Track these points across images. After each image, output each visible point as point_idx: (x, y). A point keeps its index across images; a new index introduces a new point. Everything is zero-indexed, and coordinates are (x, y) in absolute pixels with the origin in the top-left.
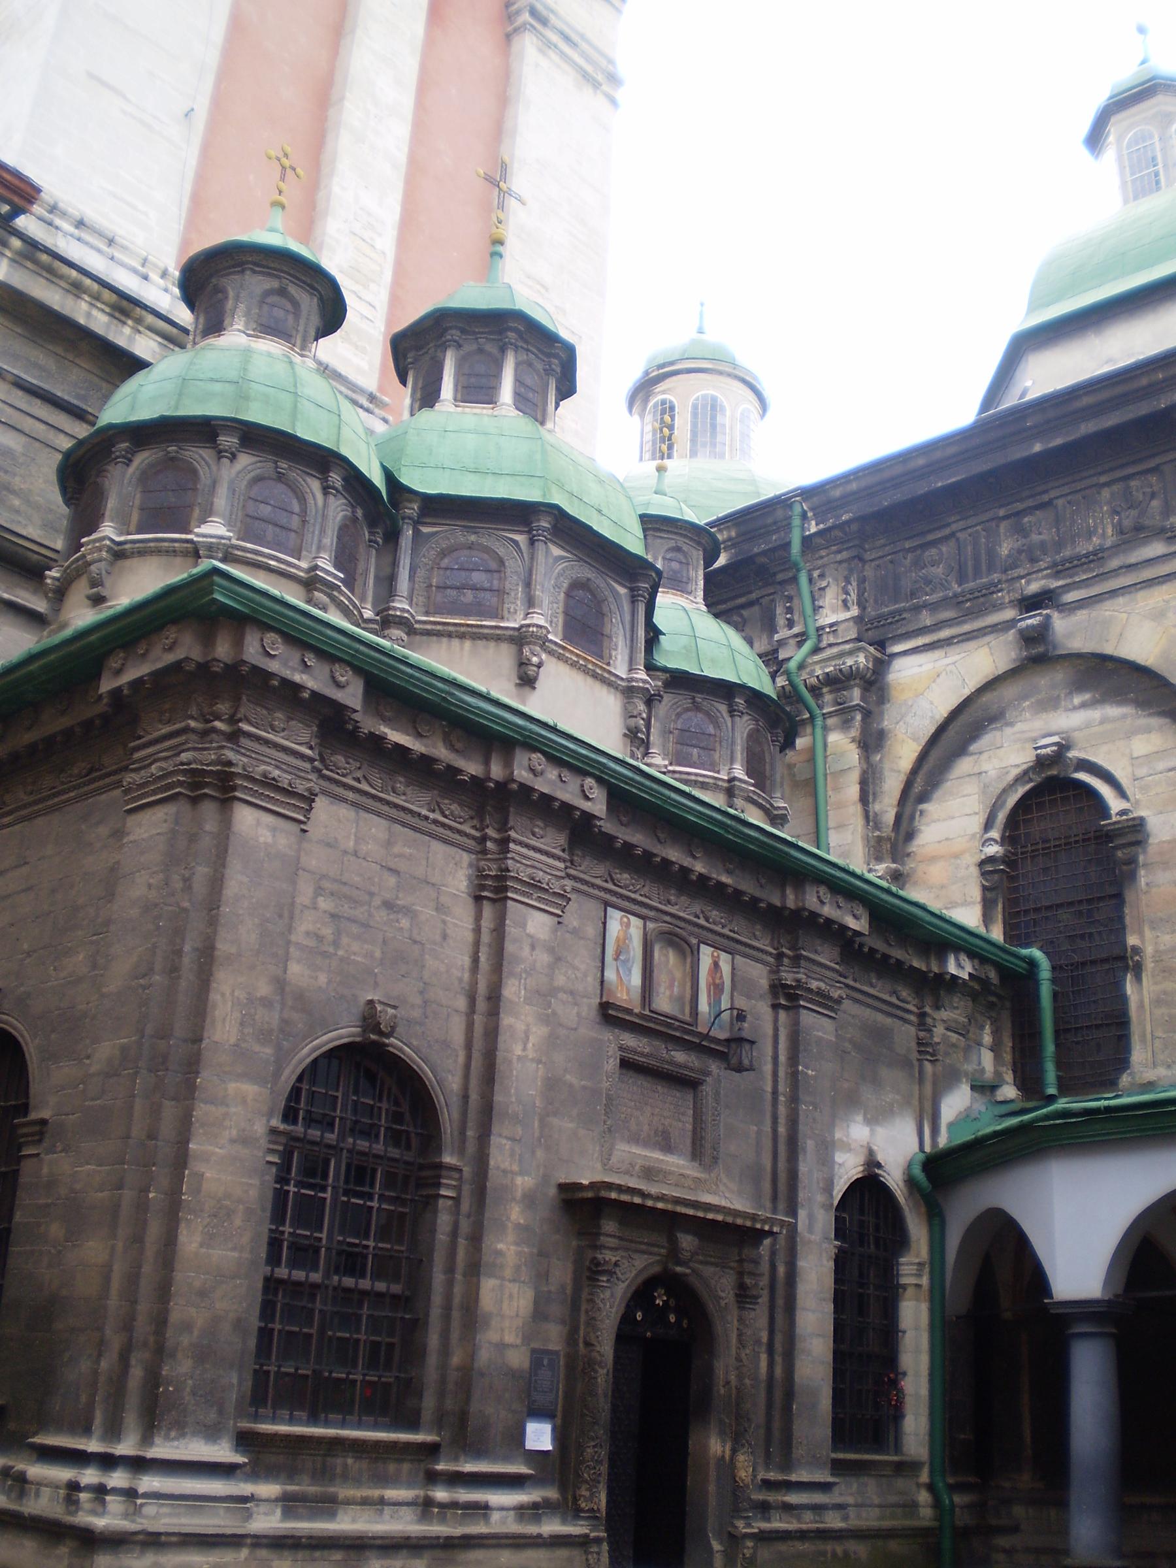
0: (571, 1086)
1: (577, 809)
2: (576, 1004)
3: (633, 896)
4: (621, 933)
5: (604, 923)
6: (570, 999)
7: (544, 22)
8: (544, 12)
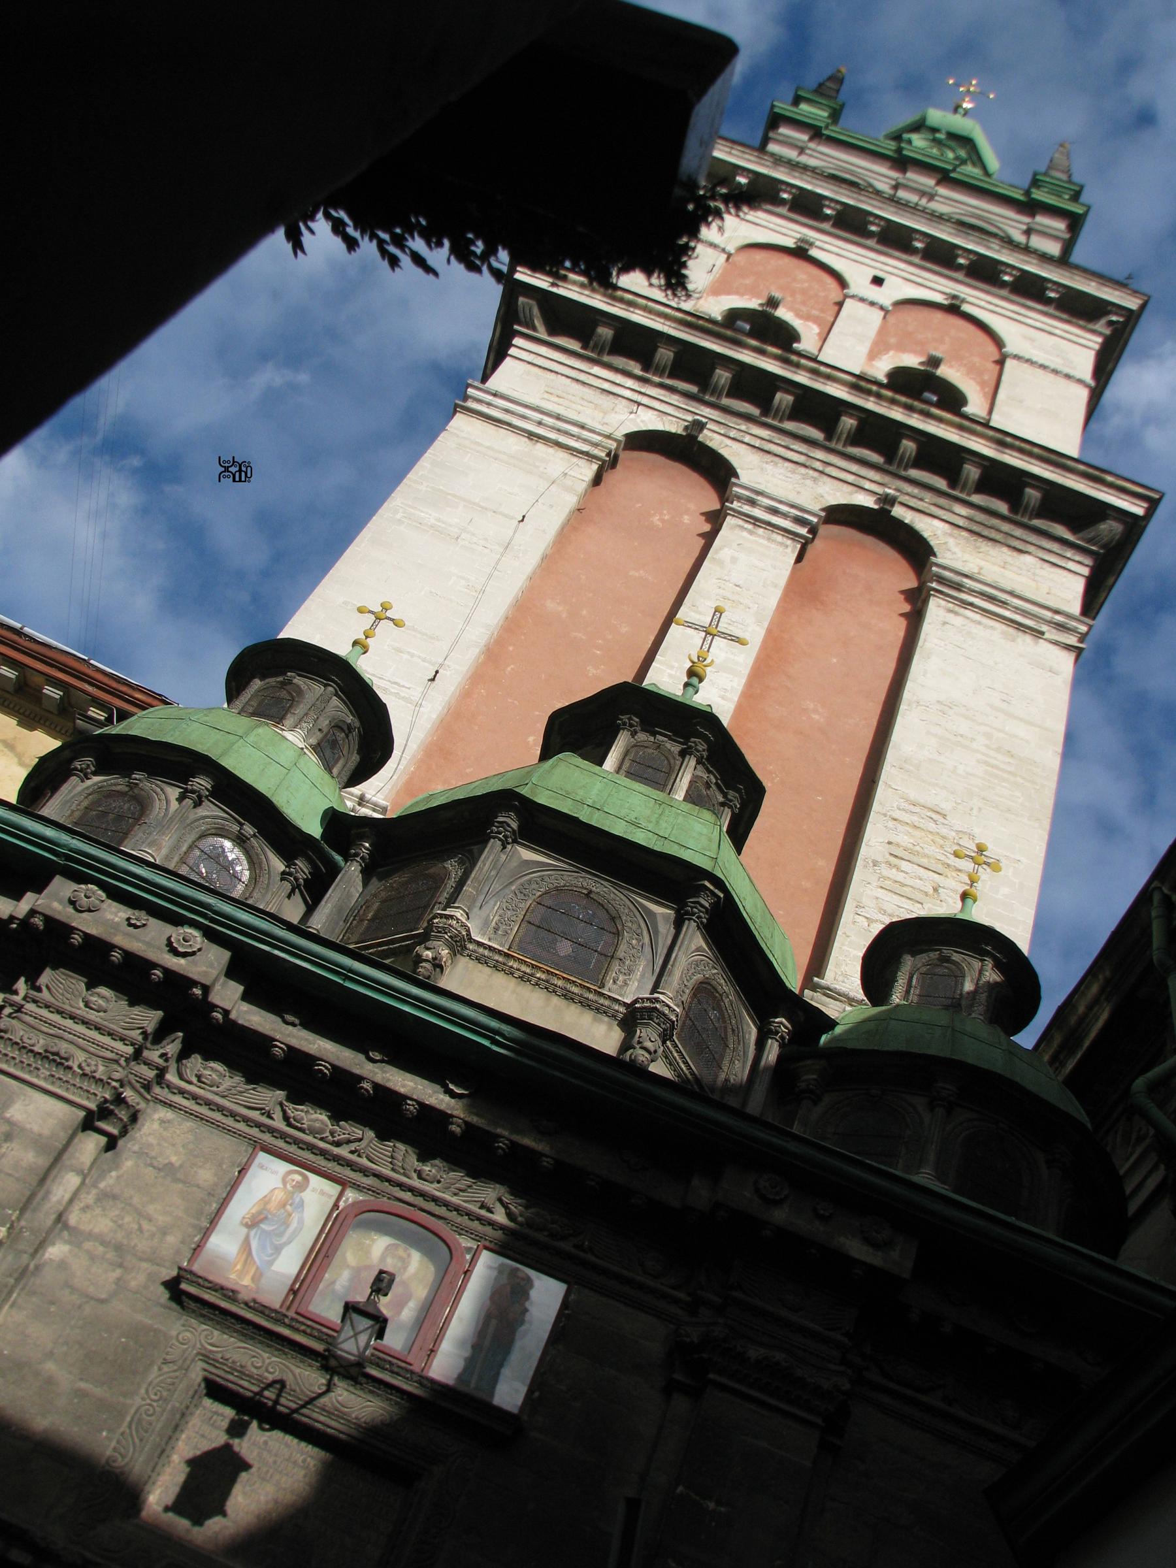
0: (50, 1381)
1: (155, 965)
2: (121, 1266)
3: (336, 1151)
4: (280, 1195)
5: (243, 1171)
6: (111, 1255)
7: (959, 587)
8: (957, 578)
